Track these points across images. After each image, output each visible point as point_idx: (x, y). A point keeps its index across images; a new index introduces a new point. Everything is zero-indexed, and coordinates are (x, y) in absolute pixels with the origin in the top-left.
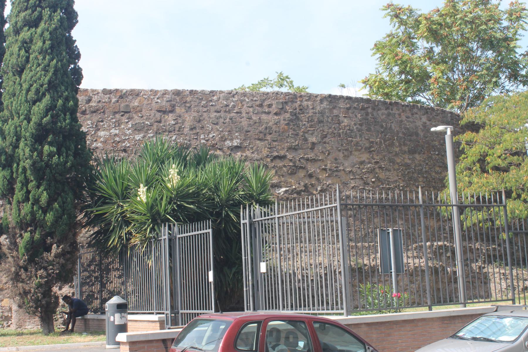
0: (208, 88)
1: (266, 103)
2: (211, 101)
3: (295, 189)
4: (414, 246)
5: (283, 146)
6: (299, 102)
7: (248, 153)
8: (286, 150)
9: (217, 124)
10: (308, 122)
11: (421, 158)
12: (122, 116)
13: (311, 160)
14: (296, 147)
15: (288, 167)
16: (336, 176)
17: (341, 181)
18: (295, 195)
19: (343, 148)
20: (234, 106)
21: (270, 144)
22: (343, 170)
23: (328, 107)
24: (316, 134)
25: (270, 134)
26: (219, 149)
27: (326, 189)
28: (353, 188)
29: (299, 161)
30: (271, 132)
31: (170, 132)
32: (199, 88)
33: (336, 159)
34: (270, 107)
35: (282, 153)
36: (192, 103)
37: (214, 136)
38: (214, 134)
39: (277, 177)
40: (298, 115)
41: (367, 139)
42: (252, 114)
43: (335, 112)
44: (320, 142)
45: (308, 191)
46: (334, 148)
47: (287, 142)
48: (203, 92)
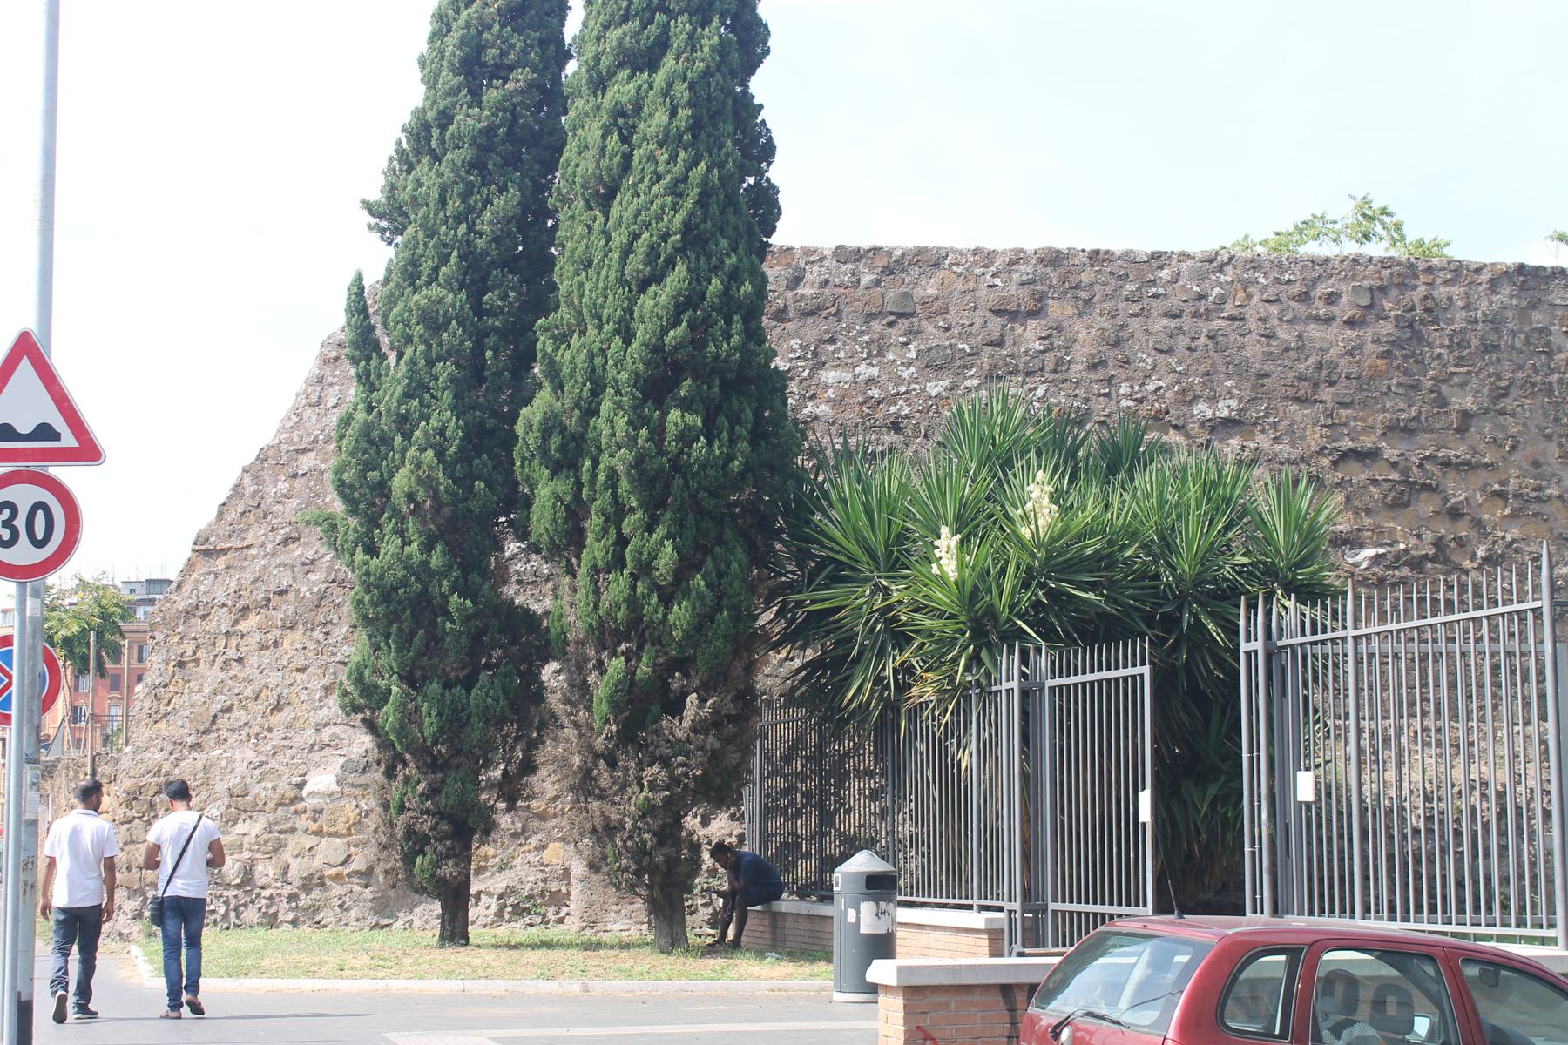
0: (1145, 245)
1: (1321, 290)
2: (1153, 282)
3: (1406, 551)
5: (1370, 421)
6: (1422, 288)
7: (1263, 441)
8: (1379, 432)
9: (1169, 351)
10: (1449, 347)
12: (890, 325)
13: (1458, 465)
14: (1412, 425)
15: (1386, 485)
16: (1536, 514)
17: (1551, 529)
18: (1406, 572)
19: (1559, 430)
20: (1222, 300)
21: (1330, 416)
22: (1560, 497)
23: (1514, 302)
24: (1474, 384)
25: (1332, 383)
26: (1176, 427)
27: (1502, 556)
29: (1420, 466)
30: (1335, 377)
31: (1028, 374)
32: (1117, 245)
33: (1536, 464)
34: (1332, 303)
35: (1367, 442)
36: (1097, 288)
37: (1159, 388)
38: (1161, 383)
39: (1349, 515)
40: (1417, 326)
42: (1276, 322)
43: (1538, 319)
44: (1487, 411)
45: (1446, 561)
46: (1533, 429)
47: (1384, 410)
48: (1129, 258)
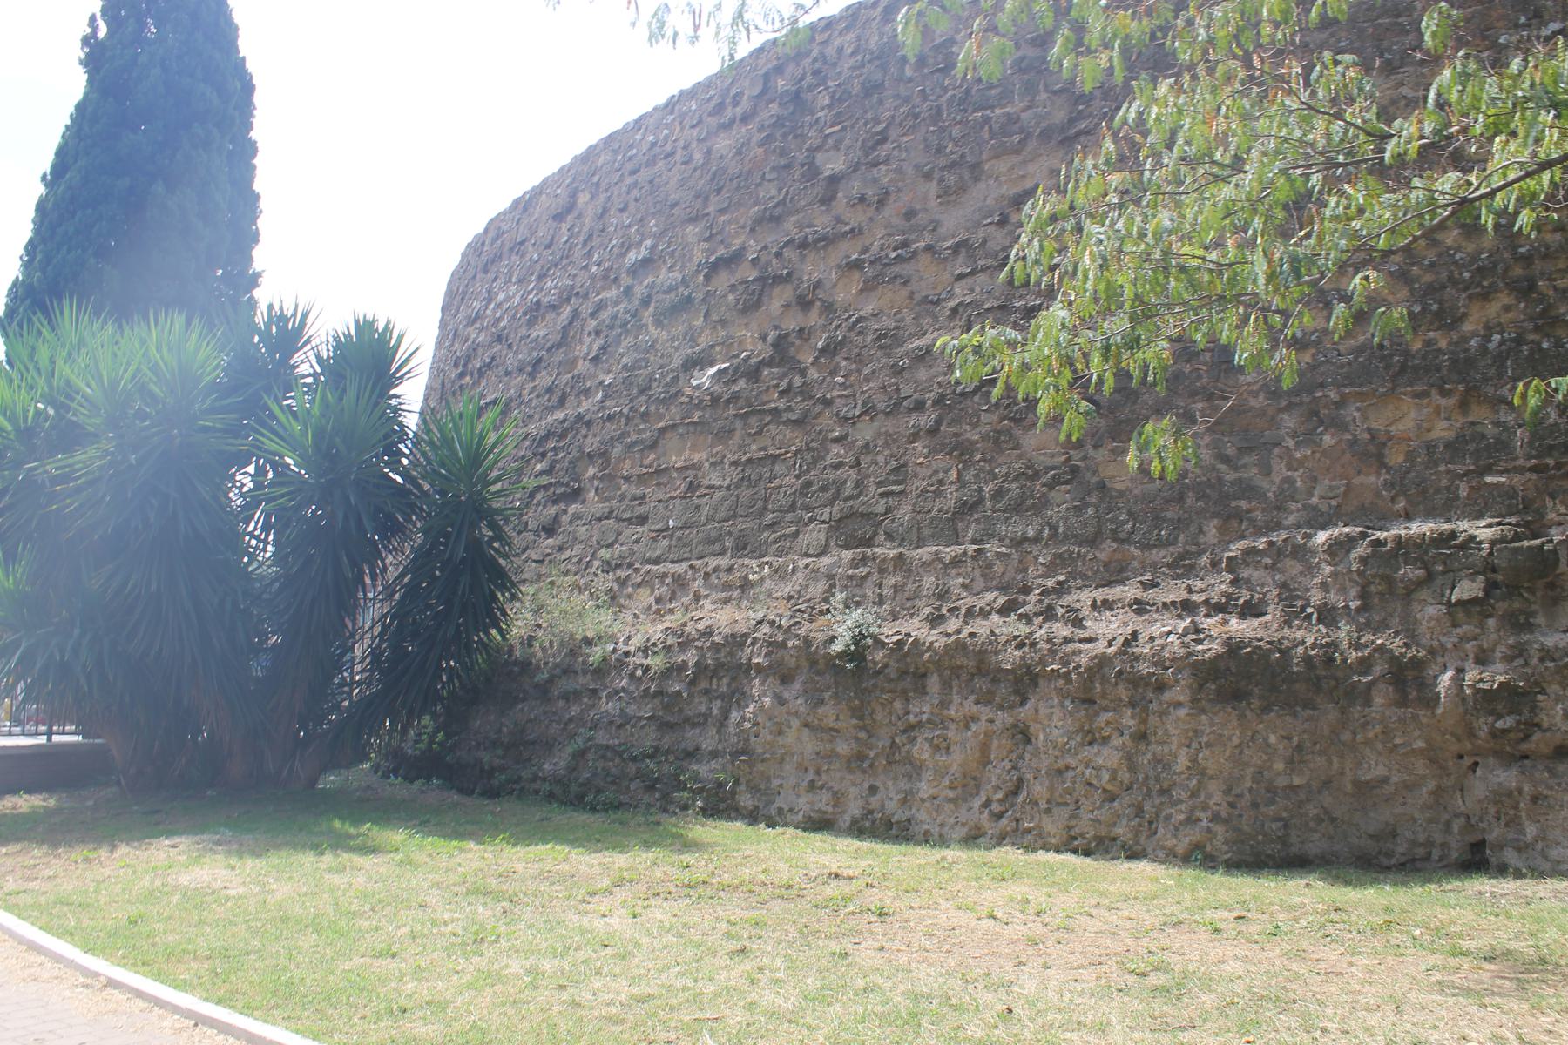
4: (1236, 548)
11: (1405, 91)
14: (779, 210)
19: (942, 162)
28: (954, 311)
29: (778, 255)
35: (736, 244)
41: (1061, 91)
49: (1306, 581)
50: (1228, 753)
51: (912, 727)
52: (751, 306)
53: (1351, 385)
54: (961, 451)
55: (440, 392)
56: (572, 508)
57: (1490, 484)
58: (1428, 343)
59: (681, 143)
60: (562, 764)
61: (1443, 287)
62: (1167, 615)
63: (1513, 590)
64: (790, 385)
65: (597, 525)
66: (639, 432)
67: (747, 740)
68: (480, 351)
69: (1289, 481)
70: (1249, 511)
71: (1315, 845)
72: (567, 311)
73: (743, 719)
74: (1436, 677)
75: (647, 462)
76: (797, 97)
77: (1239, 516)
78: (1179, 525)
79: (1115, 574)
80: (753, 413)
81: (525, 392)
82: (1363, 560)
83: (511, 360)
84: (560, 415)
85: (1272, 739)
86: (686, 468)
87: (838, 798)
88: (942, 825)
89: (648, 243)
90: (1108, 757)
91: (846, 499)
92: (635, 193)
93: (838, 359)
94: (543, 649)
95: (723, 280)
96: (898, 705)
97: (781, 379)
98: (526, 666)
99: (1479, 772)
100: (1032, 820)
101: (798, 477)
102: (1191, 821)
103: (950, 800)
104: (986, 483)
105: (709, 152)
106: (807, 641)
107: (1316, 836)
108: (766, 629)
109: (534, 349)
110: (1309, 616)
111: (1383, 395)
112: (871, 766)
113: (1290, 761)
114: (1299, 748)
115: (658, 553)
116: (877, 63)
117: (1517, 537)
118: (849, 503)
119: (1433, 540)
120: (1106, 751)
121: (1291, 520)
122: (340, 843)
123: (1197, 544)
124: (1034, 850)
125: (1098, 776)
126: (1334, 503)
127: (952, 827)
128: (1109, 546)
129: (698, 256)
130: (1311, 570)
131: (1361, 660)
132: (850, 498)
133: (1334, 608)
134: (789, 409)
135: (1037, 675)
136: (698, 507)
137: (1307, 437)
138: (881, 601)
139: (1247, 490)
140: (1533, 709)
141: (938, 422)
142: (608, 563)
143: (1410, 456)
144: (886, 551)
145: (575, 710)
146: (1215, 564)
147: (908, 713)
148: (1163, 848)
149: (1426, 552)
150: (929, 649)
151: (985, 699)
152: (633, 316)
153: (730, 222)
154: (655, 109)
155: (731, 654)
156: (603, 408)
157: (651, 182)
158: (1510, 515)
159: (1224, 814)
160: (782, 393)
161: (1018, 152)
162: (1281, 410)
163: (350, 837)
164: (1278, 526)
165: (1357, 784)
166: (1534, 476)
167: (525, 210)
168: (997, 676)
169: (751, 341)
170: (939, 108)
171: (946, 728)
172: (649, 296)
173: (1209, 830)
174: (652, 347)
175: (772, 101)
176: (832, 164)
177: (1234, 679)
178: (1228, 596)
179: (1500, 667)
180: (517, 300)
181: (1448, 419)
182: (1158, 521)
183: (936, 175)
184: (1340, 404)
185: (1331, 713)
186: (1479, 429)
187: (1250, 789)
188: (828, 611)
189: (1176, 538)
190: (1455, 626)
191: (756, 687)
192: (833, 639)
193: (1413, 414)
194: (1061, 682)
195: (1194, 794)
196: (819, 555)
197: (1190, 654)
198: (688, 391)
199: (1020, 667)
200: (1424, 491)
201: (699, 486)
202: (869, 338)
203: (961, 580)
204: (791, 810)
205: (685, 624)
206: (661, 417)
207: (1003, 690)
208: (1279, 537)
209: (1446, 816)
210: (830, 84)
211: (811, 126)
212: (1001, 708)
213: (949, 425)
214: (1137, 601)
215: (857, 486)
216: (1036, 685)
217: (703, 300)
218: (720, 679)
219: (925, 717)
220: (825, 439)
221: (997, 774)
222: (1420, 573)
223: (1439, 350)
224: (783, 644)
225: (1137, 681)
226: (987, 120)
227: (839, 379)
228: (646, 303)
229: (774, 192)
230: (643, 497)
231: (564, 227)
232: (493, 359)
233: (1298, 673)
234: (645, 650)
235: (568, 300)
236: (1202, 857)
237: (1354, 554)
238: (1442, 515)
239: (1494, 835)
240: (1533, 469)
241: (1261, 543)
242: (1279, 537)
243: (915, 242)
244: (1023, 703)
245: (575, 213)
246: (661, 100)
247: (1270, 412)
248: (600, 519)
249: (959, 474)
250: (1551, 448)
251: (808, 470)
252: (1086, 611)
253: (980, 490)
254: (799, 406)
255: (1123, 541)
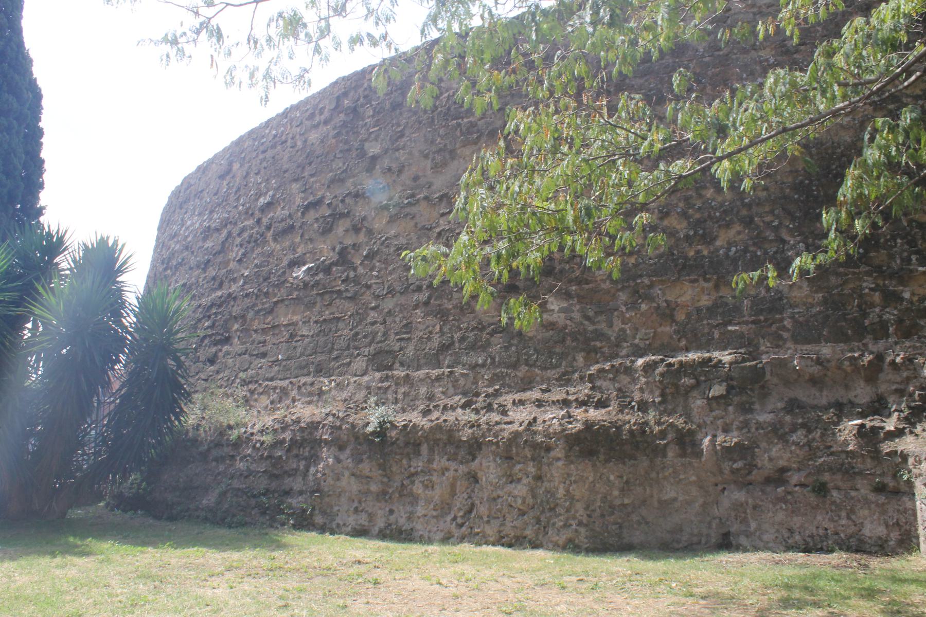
4: (593, 369)
19: (434, 149)
28: (439, 234)
29: (343, 201)
35: (319, 194)
49: (632, 387)
50: (587, 486)
51: (412, 475)
52: (327, 230)
53: (656, 276)
54: (442, 314)
55: (154, 278)
56: (225, 348)
57: (731, 331)
58: (698, 252)
59: (291, 135)
60: (213, 500)
61: (705, 221)
62: (554, 408)
63: (742, 390)
64: (347, 276)
65: (239, 359)
66: (263, 304)
67: (319, 484)
68: (176, 255)
69: (623, 330)
70: (601, 348)
71: (637, 537)
72: (225, 232)
73: (317, 471)
74: (701, 440)
75: (267, 321)
76: (355, 110)
77: (596, 350)
78: (562, 356)
79: (527, 385)
80: (327, 292)
81: (200, 280)
82: (662, 375)
83: (193, 261)
84: (219, 293)
85: (612, 478)
86: (289, 325)
87: (371, 517)
88: (430, 532)
89: (271, 193)
90: (521, 490)
91: (378, 343)
92: (264, 164)
93: (374, 261)
94: (205, 431)
95: (312, 215)
96: (405, 462)
97: (343, 273)
98: (195, 441)
99: (726, 493)
100: (479, 527)
101: (351, 330)
102: (566, 526)
103: (434, 517)
104: (456, 333)
105: (305, 141)
106: (353, 426)
107: (638, 533)
108: (330, 419)
109: (205, 254)
110: (633, 407)
111: (674, 281)
112: (390, 498)
113: (622, 490)
114: (627, 482)
115: (272, 374)
116: (399, 92)
117: (744, 360)
118: (379, 345)
119: (699, 362)
120: (519, 487)
121: (624, 352)
122: (70, 550)
123: (572, 367)
124: (480, 545)
125: (515, 501)
126: (647, 342)
127: (435, 533)
128: (524, 368)
129: (298, 201)
130: (634, 381)
131: (661, 432)
132: (381, 342)
133: (647, 402)
134: (347, 290)
135: (481, 443)
136: (295, 348)
137: (633, 306)
138: (396, 401)
139: (600, 335)
140: (753, 456)
141: (429, 298)
142: (244, 380)
143: (688, 315)
144: (400, 373)
145: (222, 468)
146: (582, 378)
147: (410, 467)
148: (552, 542)
149: (696, 369)
150: (422, 429)
151: (453, 458)
152: (261, 236)
153: (316, 182)
154: (277, 115)
155: (311, 433)
156: (243, 290)
157: (273, 158)
158: (741, 348)
159: (585, 521)
160: (343, 281)
161: (476, 143)
162: (619, 290)
163: (77, 546)
164: (617, 356)
165: (660, 502)
166: (753, 326)
167: (204, 172)
168: (459, 444)
169: (326, 251)
170: (433, 118)
171: (431, 475)
172: (271, 224)
173: (576, 531)
174: (271, 254)
175: (341, 112)
176: (374, 149)
177: (590, 444)
178: (589, 396)
179: (735, 433)
180: (197, 225)
181: (709, 294)
182: (551, 354)
183: (431, 156)
184: (651, 286)
185: (644, 462)
186: (725, 300)
187: (600, 507)
188: (366, 408)
189: (561, 364)
190: (711, 411)
191: (325, 452)
192: (368, 424)
193: (690, 292)
194: (494, 447)
195: (568, 511)
196: (362, 375)
197: (564, 430)
198: (291, 280)
199: (472, 439)
200: (696, 335)
201: (296, 335)
202: (392, 249)
203: (441, 389)
204: (344, 525)
205: (286, 416)
206: (275, 295)
207: (462, 453)
208: (617, 362)
209: (709, 519)
210: (373, 103)
211: (362, 127)
212: (462, 463)
213: (435, 300)
214: (538, 400)
215: (384, 335)
216: (481, 449)
217: (301, 227)
218: (304, 448)
219: (419, 469)
220: (367, 307)
221: (460, 502)
222: (693, 381)
223: (704, 256)
224: (340, 428)
225: (535, 446)
226: (459, 125)
227: (375, 273)
228: (268, 228)
229: (341, 165)
230: (265, 341)
231: (225, 183)
232: (183, 260)
233: (626, 440)
234: (261, 432)
235: (226, 225)
236: (573, 547)
237: (658, 371)
238: (704, 349)
239: (734, 528)
240: (753, 322)
241: (607, 366)
242: (617, 362)
243: (418, 194)
244: (473, 460)
245: (231, 175)
246: (281, 110)
247: (613, 291)
248: (240, 355)
249: (441, 329)
250: (762, 310)
251: (357, 326)
252: (509, 406)
253: (452, 337)
254: (352, 289)
255: (531, 366)
